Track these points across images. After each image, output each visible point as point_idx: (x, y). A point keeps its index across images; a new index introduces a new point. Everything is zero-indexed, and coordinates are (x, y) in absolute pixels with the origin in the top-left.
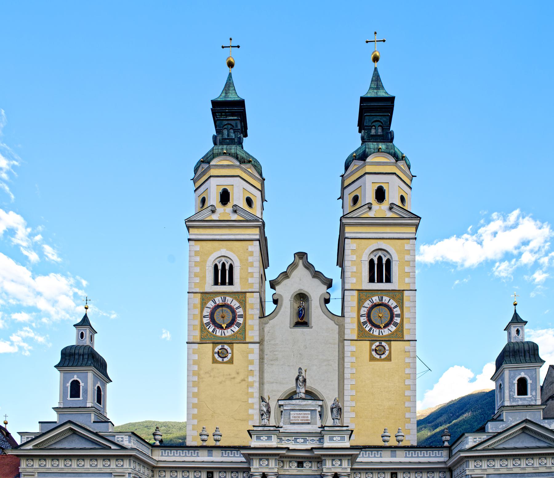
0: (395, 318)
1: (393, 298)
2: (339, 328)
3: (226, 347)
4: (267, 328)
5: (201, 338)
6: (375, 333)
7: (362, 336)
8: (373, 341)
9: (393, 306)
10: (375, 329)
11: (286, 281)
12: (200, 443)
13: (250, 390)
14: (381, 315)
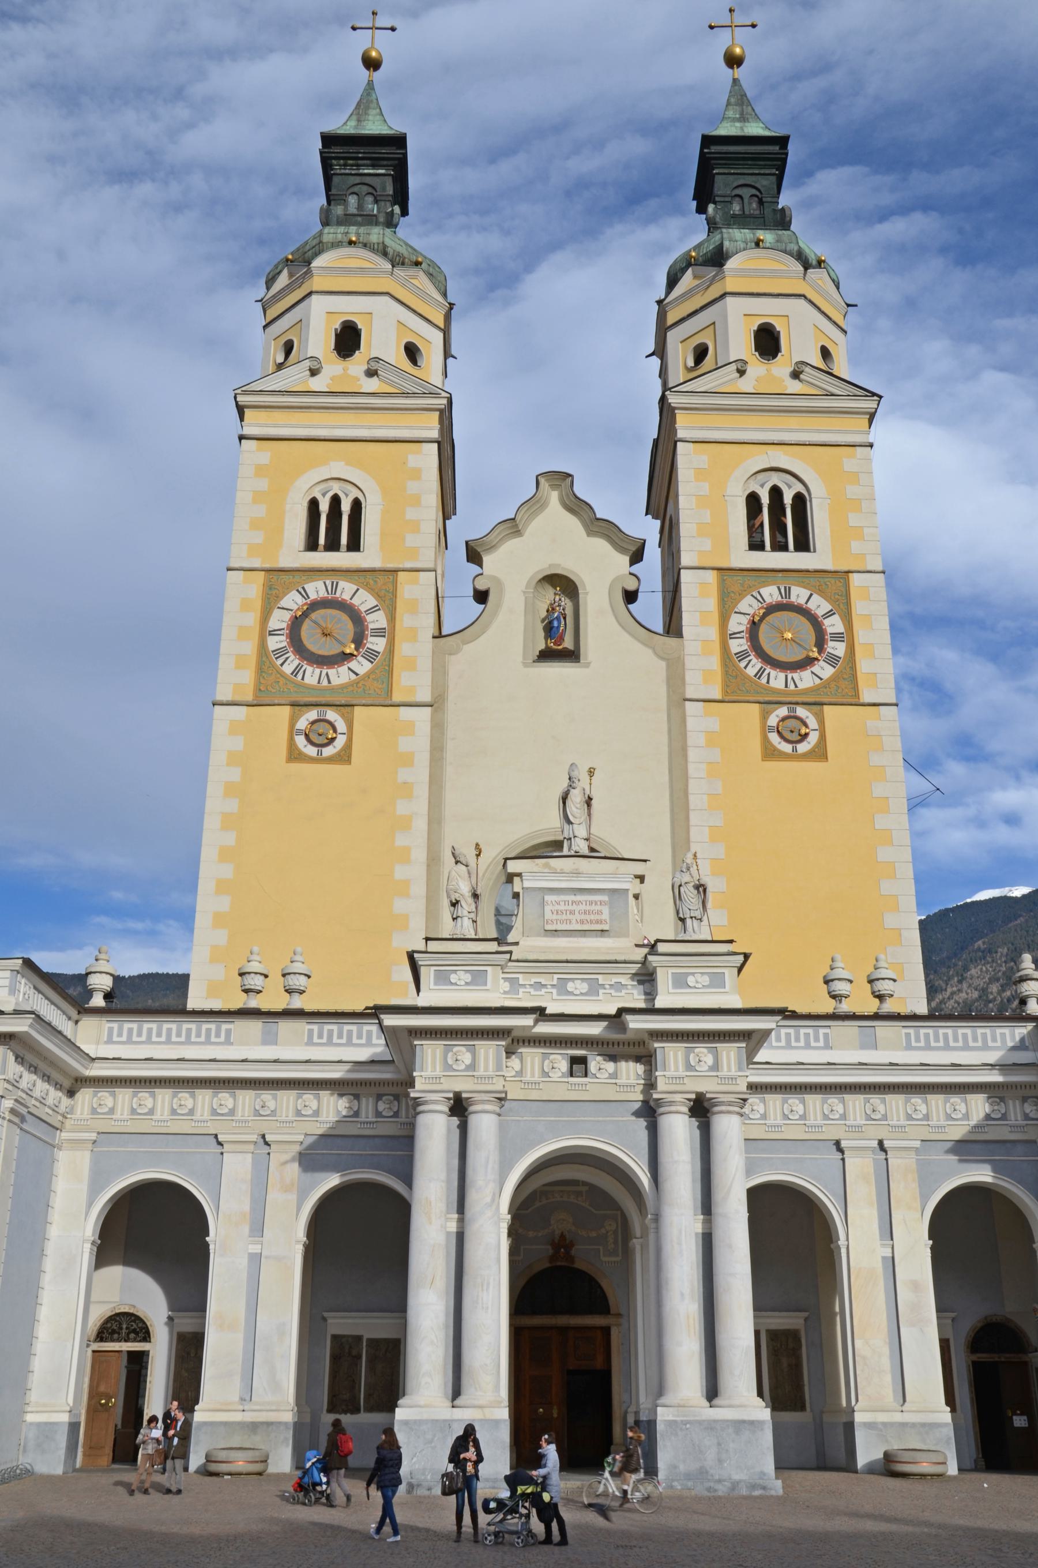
0: (831, 644)
1: (822, 593)
2: (668, 667)
3: (331, 715)
4: (457, 665)
5: (258, 690)
6: (773, 684)
7: (735, 689)
8: (769, 704)
9: (820, 612)
10: (773, 673)
11: (512, 545)
12: (239, 1001)
13: (401, 841)
14: (787, 636)
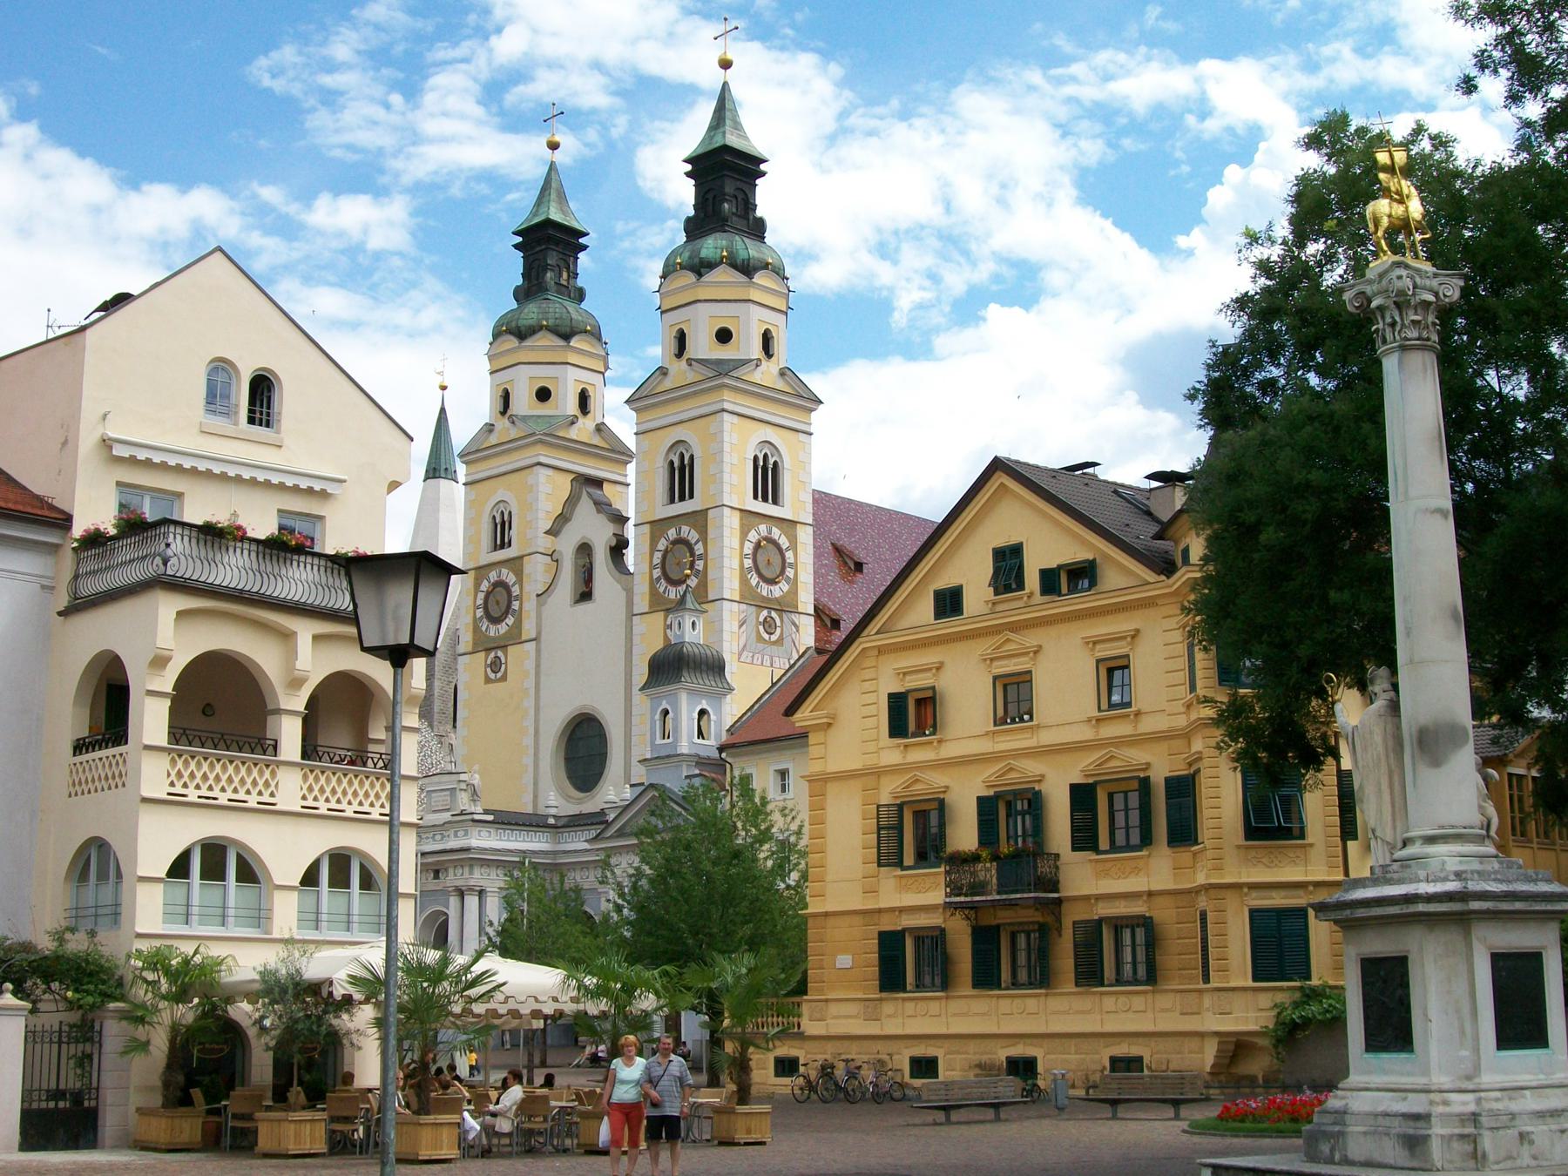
3: (500, 654)
4: (546, 610)
